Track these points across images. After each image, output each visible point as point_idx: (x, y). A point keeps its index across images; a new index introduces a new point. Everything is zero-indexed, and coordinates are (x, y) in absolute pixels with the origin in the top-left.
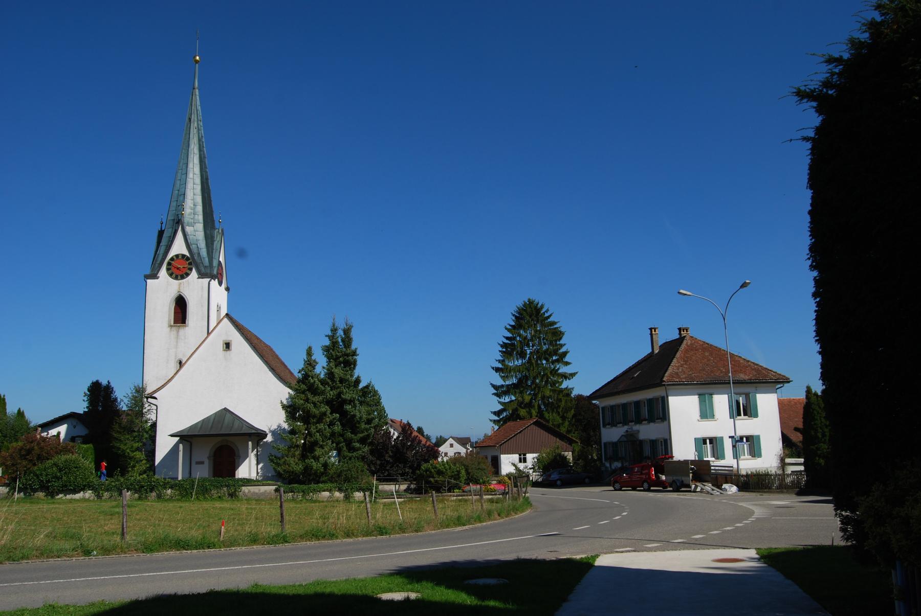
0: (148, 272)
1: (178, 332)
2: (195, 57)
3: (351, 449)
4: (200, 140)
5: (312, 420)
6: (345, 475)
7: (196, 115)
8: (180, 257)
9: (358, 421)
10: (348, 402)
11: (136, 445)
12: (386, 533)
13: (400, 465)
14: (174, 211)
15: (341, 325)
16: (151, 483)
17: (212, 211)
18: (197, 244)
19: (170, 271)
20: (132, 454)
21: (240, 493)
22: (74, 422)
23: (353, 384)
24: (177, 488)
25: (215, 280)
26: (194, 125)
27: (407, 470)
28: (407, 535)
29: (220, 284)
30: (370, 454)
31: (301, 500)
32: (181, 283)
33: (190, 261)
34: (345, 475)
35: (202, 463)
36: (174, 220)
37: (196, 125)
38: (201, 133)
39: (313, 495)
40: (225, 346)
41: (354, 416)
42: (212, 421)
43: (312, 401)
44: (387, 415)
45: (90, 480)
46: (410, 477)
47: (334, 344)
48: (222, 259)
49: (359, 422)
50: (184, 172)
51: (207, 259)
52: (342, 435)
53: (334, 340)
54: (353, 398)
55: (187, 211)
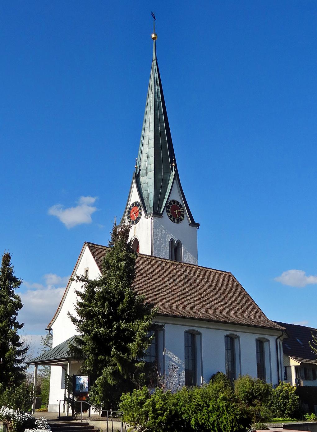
4: (155, 101)
37: (153, 90)
55: (143, 164)
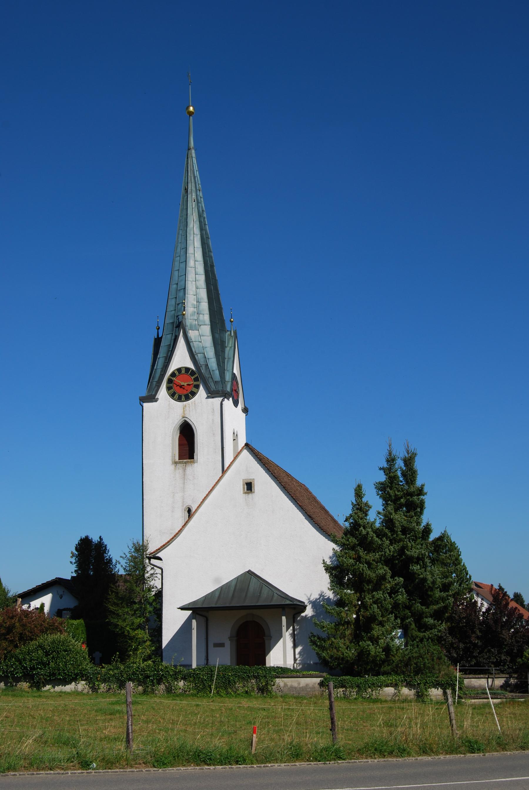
0: (144, 393)
1: (185, 470)
2: (188, 107)
3: (422, 627)
4: (200, 216)
5: (367, 587)
6: (416, 664)
7: (193, 184)
8: (183, 372)
9: (429, 587)
10: (415, 560)
11: (138, 621)
12: (479, 750)
13: (493, 650)
14: (173, 312)
15: (400, 453)
16: (158, 672)
17: (220, 309)
18: (204, 354)
19: (172, 391)
20: (133, 634)
21: (273, 687)
22: (60, 590)
23: (420, 535)
24: (192, 679)
25: (228, 399)
26: (192, 196)
27: (503, 657)
28: (509, 753)
29: (236, 404)
30: (449, 634)
31: (355, 699)
32: (185, 406)
33: (196, 376)
34: (416, 664)
35: (222, 645)
36: (173, 323)
37: (194, 196)
38: (202, 207)
39: (372, 691)
40: (246, 487)
41: (425, 580)
42: (232, 589)
43: (366, 559)
44: (470, 577)
45: (83, 668)
46: (509, 668)
47: (392, 479)
48: (236, 371)
49: (431, 589)
50: (183, 259)
51: (217, 372)
52: (409, 607)
53: (392, 475)
54: (422, 554)
55: (190, 310)
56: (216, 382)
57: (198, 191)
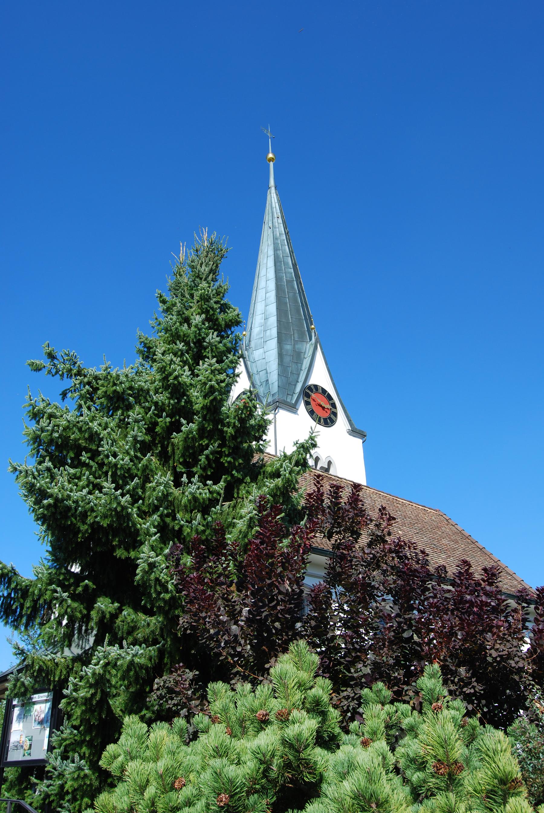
4: (275, 239)
7: (270, 215)
37: (271, 225)
56: (273, 395)
57: (276, 219)
